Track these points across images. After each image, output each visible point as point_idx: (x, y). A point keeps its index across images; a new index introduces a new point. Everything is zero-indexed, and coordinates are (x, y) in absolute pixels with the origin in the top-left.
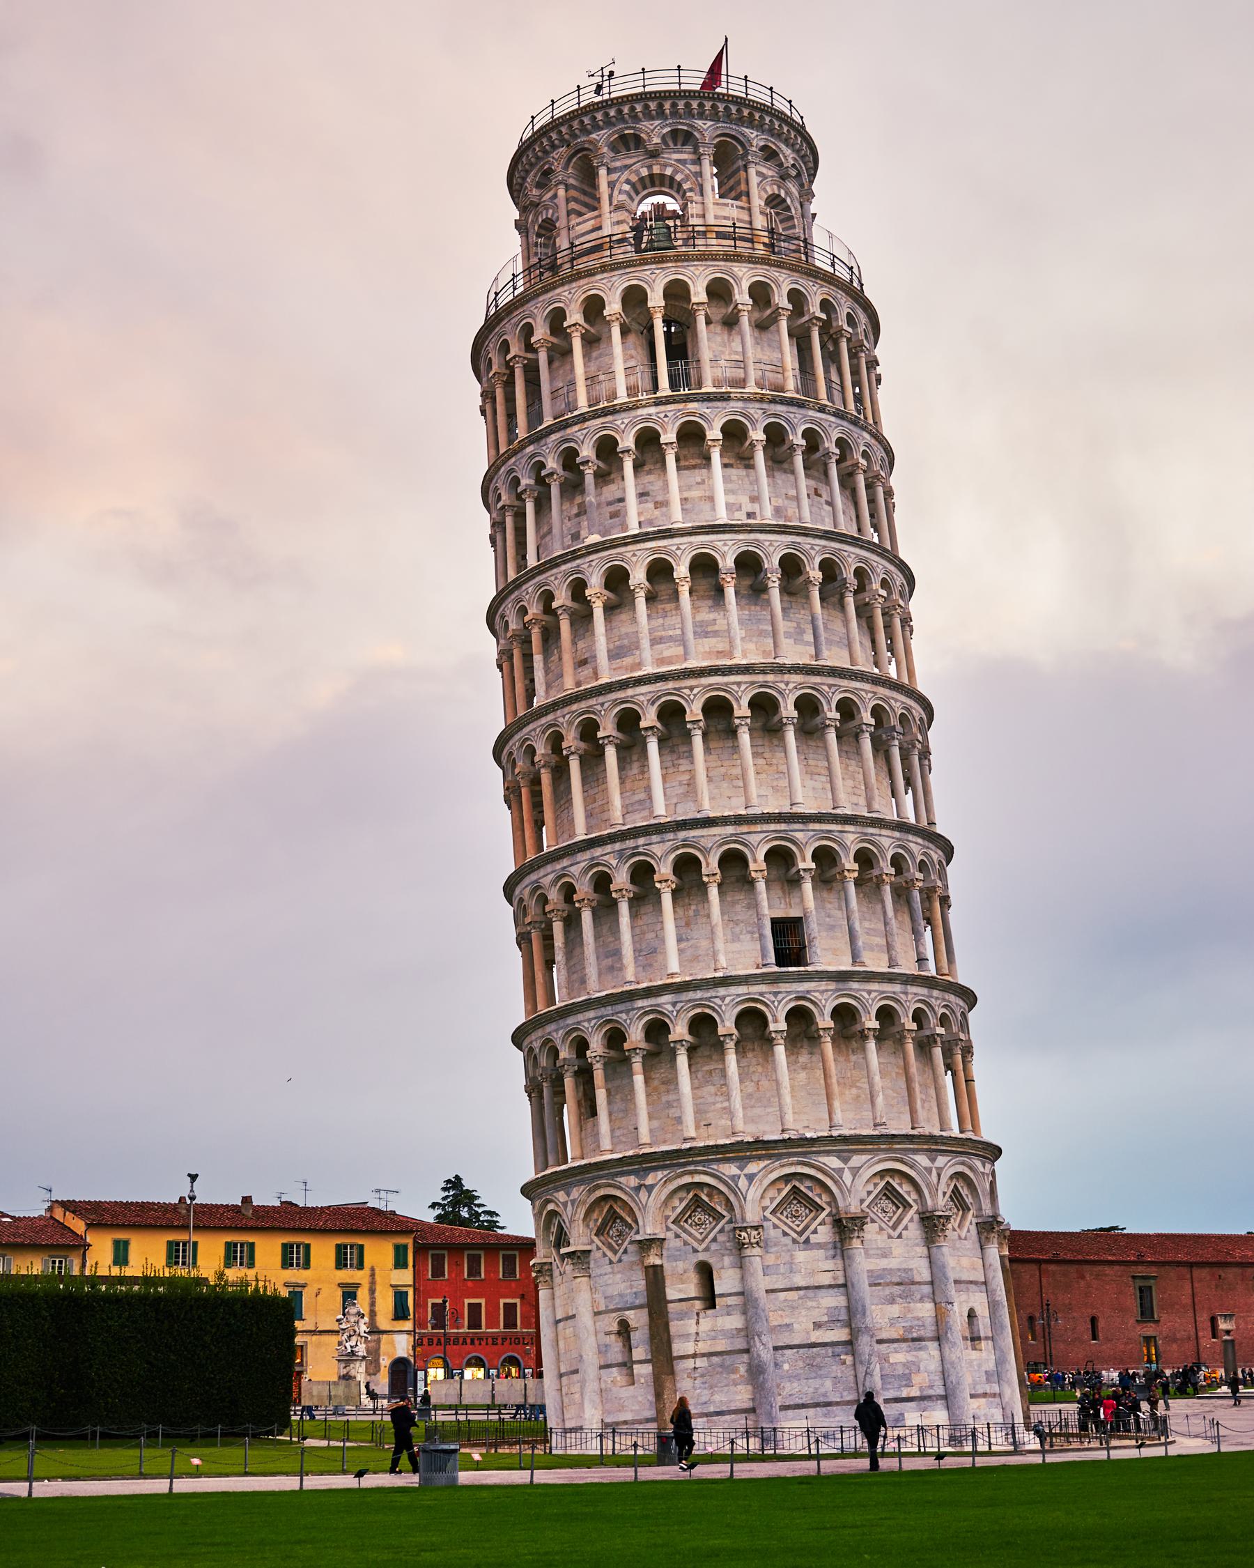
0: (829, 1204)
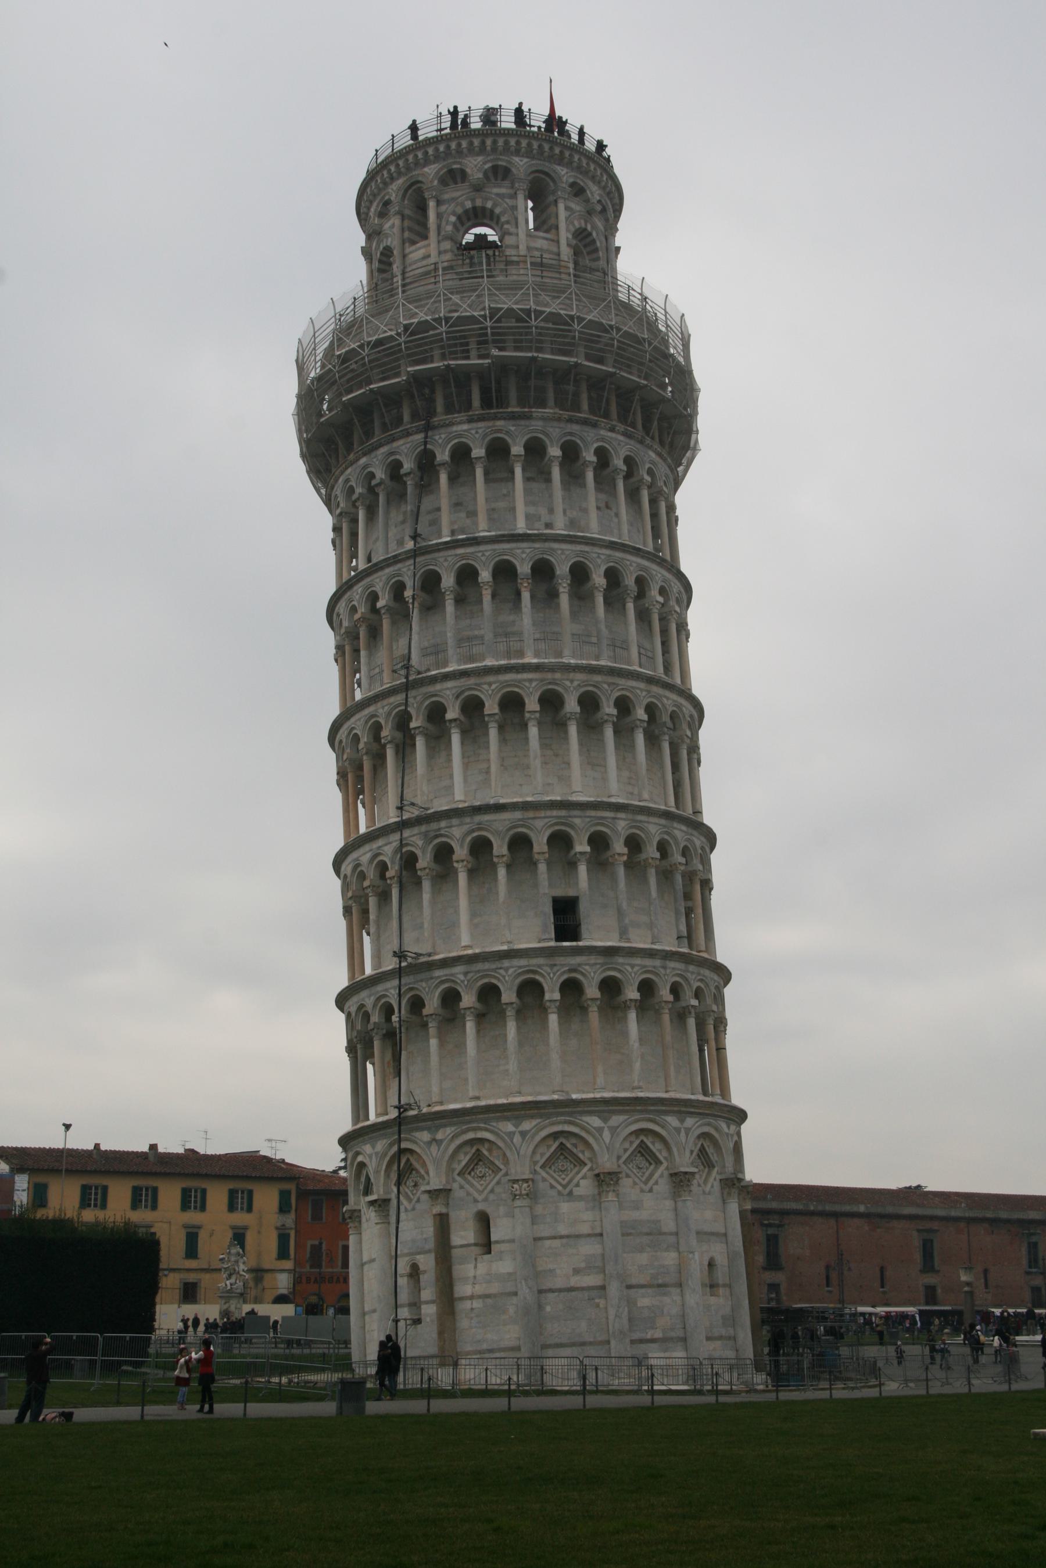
0: (590, 1159)
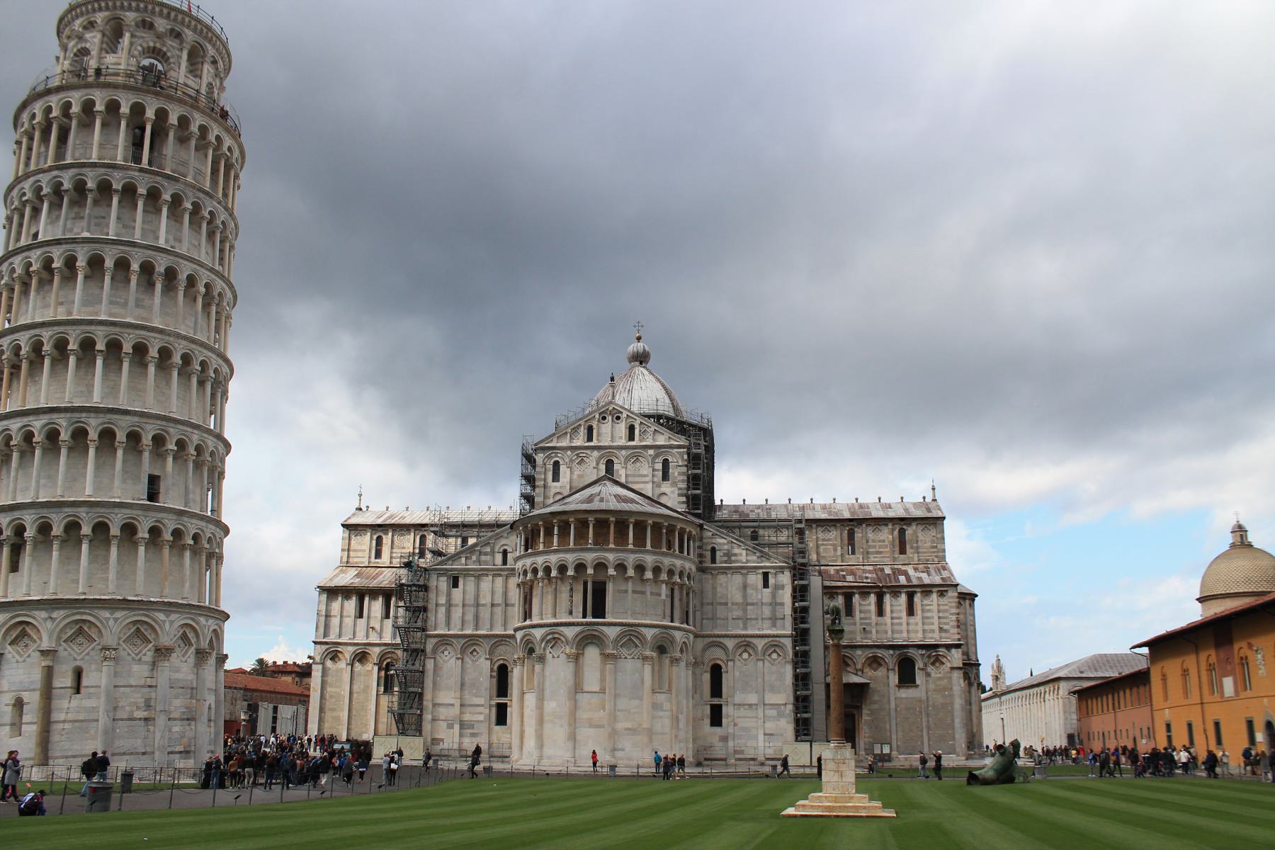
0: (154, 639)
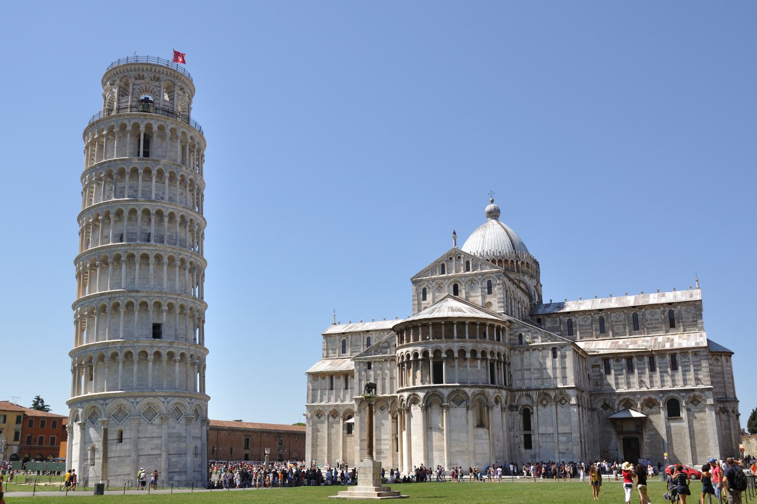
0: (160, 412)
